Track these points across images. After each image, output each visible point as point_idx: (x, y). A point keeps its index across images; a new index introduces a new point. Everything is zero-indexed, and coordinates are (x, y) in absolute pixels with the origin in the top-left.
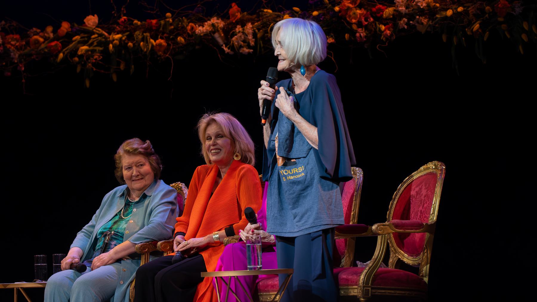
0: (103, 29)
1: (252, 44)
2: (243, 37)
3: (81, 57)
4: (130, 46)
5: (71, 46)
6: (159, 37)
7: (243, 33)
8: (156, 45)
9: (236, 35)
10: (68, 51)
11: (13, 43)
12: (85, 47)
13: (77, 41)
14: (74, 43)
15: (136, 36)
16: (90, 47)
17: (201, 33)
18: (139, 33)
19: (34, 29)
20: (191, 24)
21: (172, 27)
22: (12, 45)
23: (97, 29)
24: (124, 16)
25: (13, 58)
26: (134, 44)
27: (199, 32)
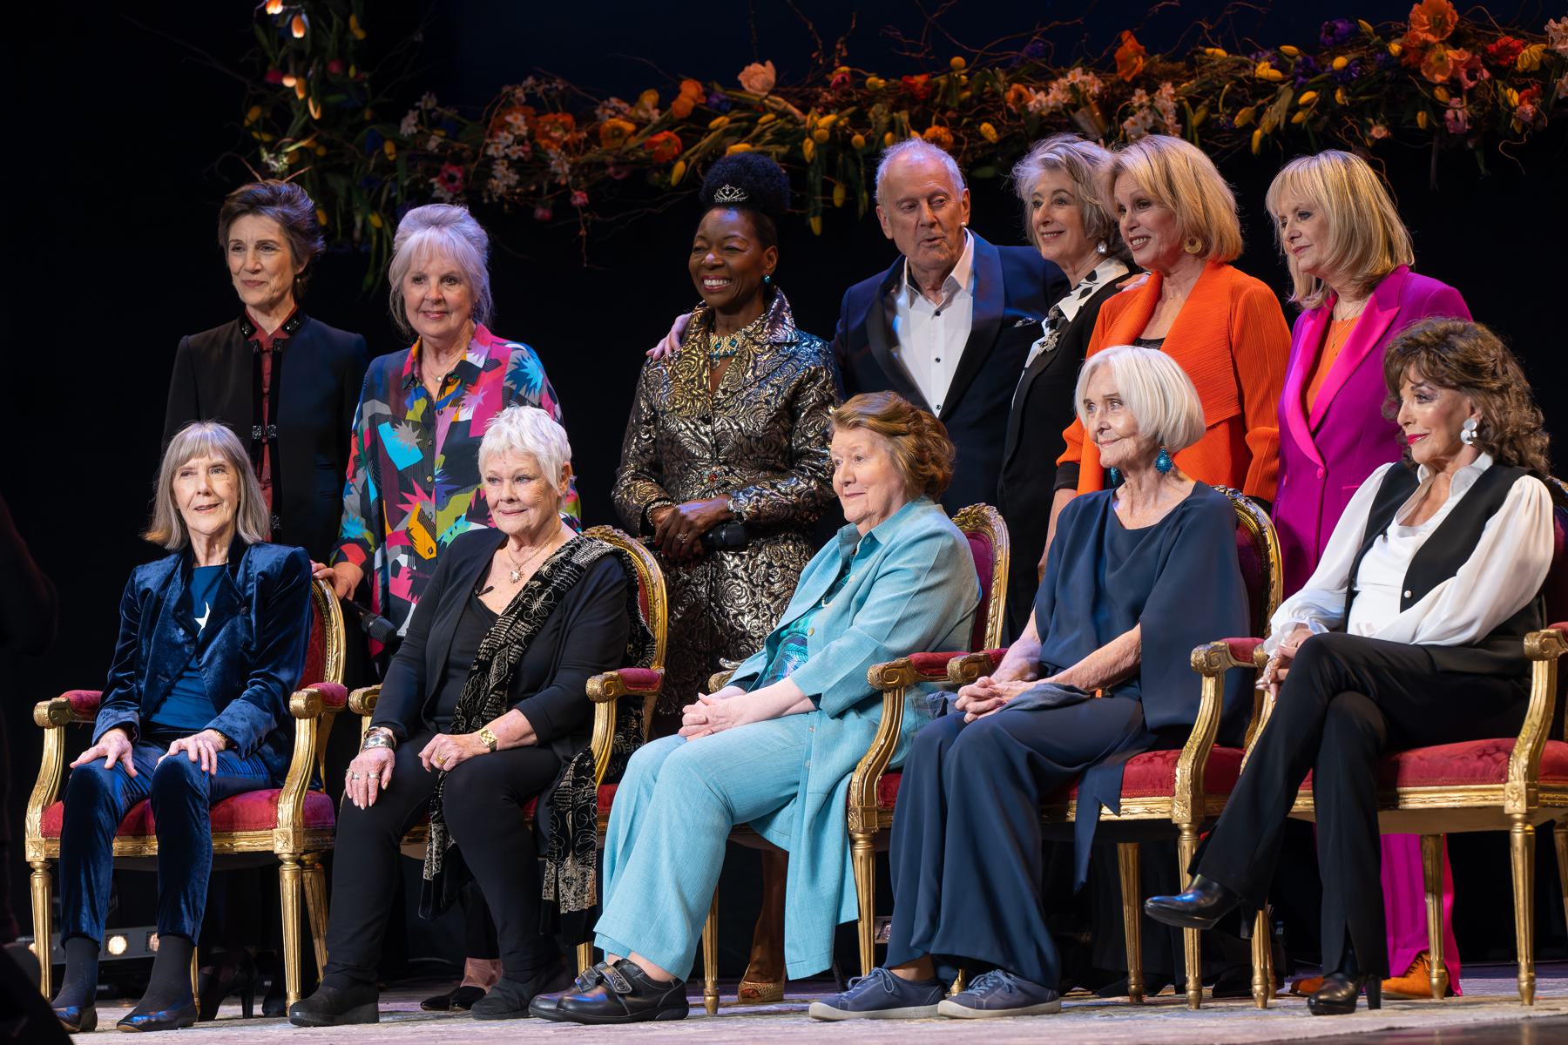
0: (787, 100)
2: (1150, 120)
4: (857, 142)
5: (705, 141)
6: (934, 118)
7: (1151, 108)
9: (1132, 114)
10: (696, 156)
11: (556, 134)
12: (742, 147)
13: (721, 130)
14: (713, 135)
15: (876, 117)
16: (753, 146)
18: (881, 110)
19: (614, 101)
20: (1015, 86)
21: (968, 94)
22: (552, 140)
23: (772, 97)
24: (841, 65)
25: (555, 174)
26: (866, 139)
27: (1037, 105)
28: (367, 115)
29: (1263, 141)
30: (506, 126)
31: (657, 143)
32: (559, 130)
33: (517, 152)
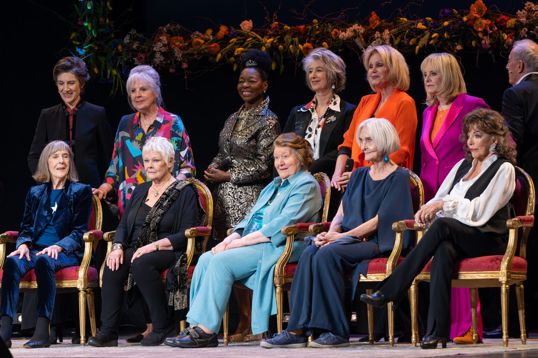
0: (256, 33)
3: (237, 57)
4: (280, 48)
5: (228, 47)
7: (381, 38)
9: (375, 40)
10: (225, 52)
12: (241, 49)
15: (287, 39)
16: (245, 49)
17: (344, 38)
19: (197, 32)
20: (335, 30)
21: (318, 32)
22: (175, 45)
23: (251, 32)
24: (275, 22)
25: (177, 57)
27: (342, 36)
28: (113, 36)
29: (420, 50)
30: (160, 41)
31: (212, 47)
32: (178, 42)
33: (164, 49)
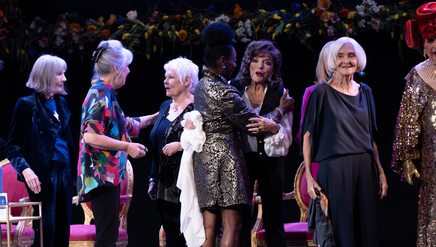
1: (250, 35)
5: (117, 32)
6: (182, 28)
7: (244, 27)
8: (180, 34)
9: (239, 28)
12: (127, 35)
14: (119, 31)
19: (91, 20)
20: (206, 19)
24: (156, 11)
29: (276, 36)
